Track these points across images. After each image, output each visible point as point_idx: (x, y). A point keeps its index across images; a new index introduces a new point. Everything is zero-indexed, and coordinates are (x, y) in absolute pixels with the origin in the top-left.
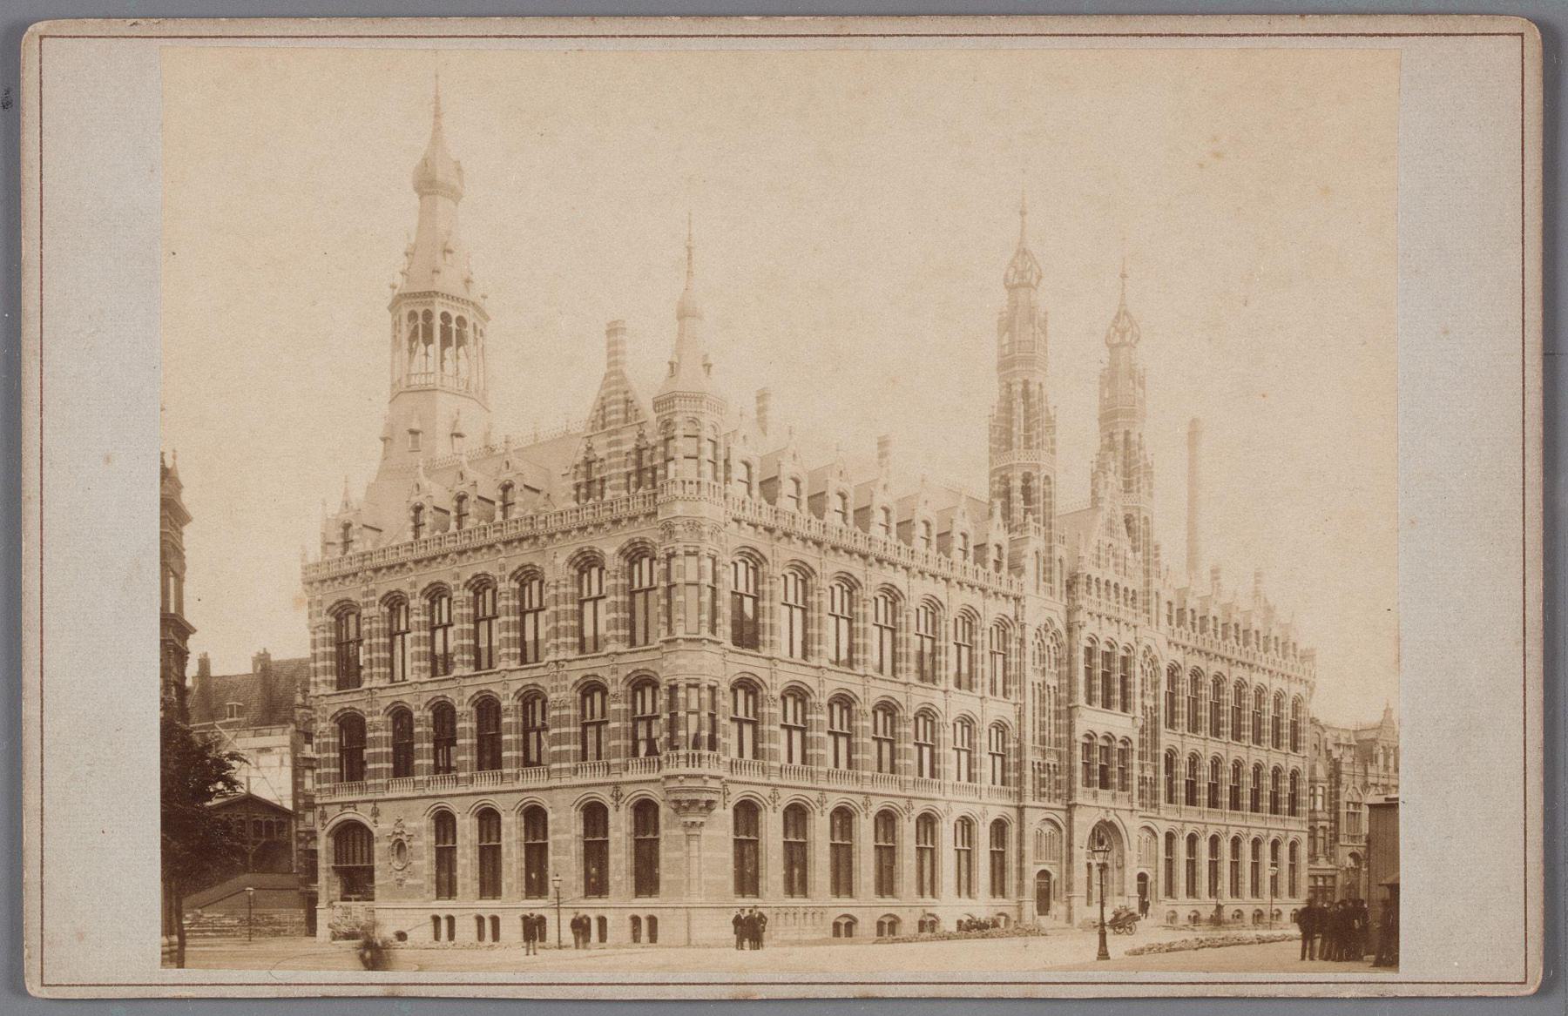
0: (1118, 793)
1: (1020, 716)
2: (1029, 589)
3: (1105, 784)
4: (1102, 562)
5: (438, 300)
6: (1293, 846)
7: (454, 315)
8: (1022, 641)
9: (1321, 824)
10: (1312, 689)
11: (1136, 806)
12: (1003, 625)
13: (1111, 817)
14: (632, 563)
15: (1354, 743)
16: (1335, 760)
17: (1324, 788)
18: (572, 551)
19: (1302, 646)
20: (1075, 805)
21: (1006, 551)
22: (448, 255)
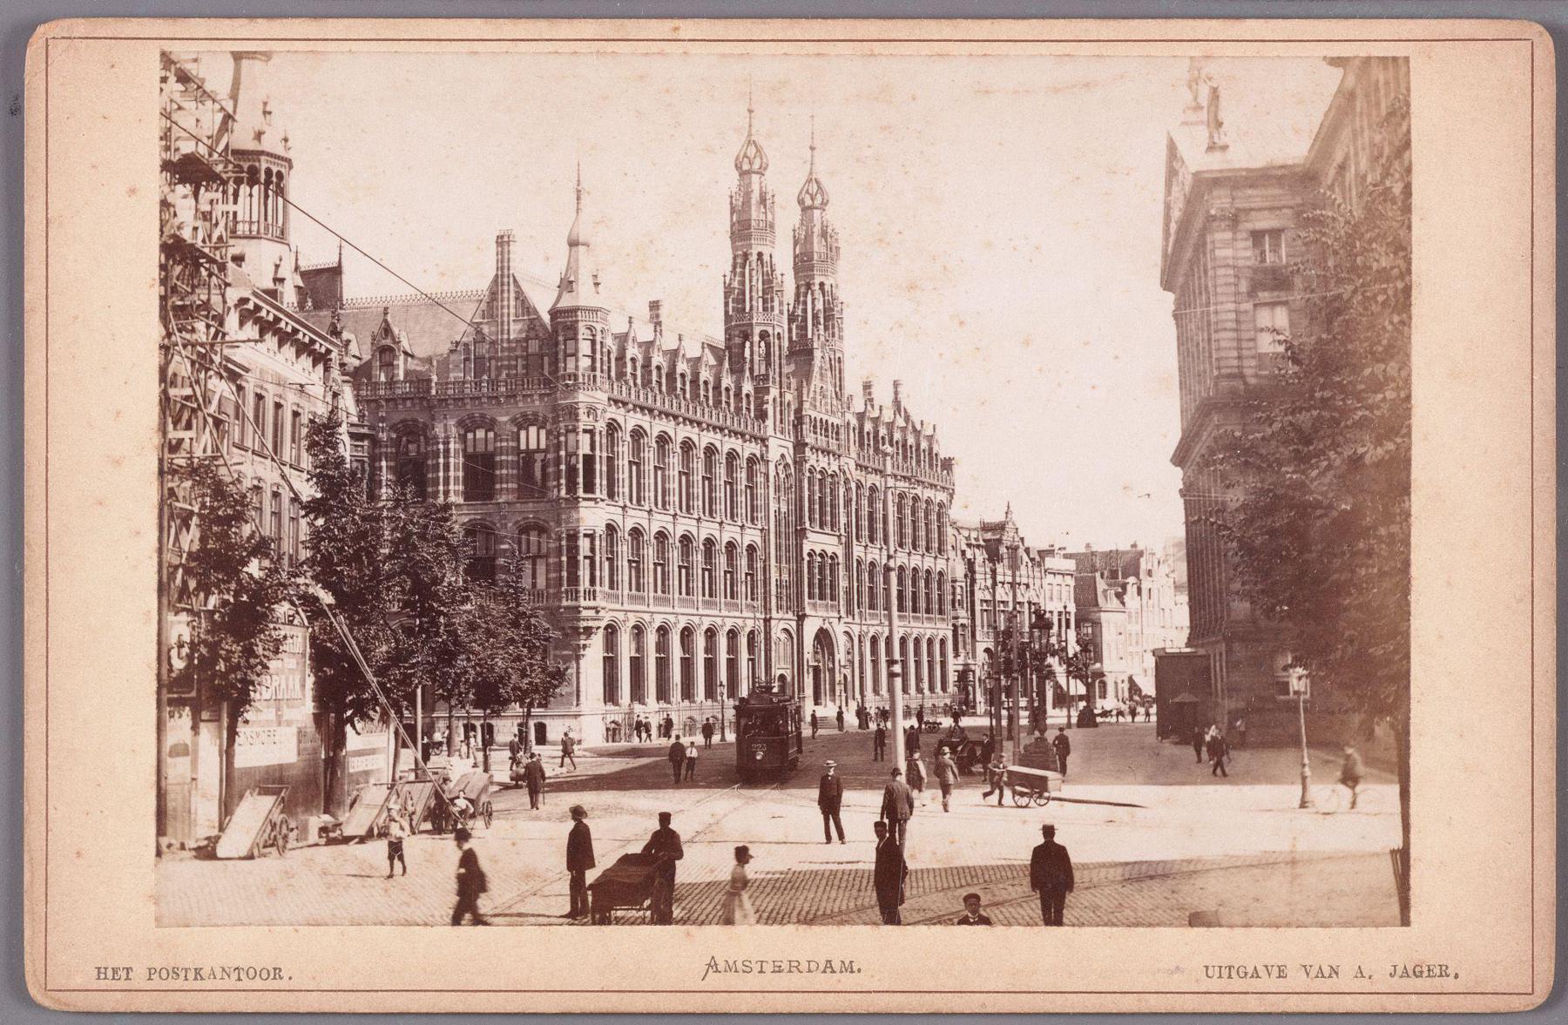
0: (818, 602)
1: (766, 541)
2: (770, 431)
3: (822, 597)
4: (818, 404)
5: (263, 158)
6: (943, 642)
7: (275, 169)
8: (767, 476)
9: (961, 621)
10: (951, 496)
11: (843, 613)
12: (752, 461)
13: (826, 626)
14: (520, 429)
15: (982, 543)
16: (969, 560)
17: (961, 587)
18: (464, 414)
19: (942, 456)
20: (805, 616)
21: (752, 399)
22: (268, 116)
